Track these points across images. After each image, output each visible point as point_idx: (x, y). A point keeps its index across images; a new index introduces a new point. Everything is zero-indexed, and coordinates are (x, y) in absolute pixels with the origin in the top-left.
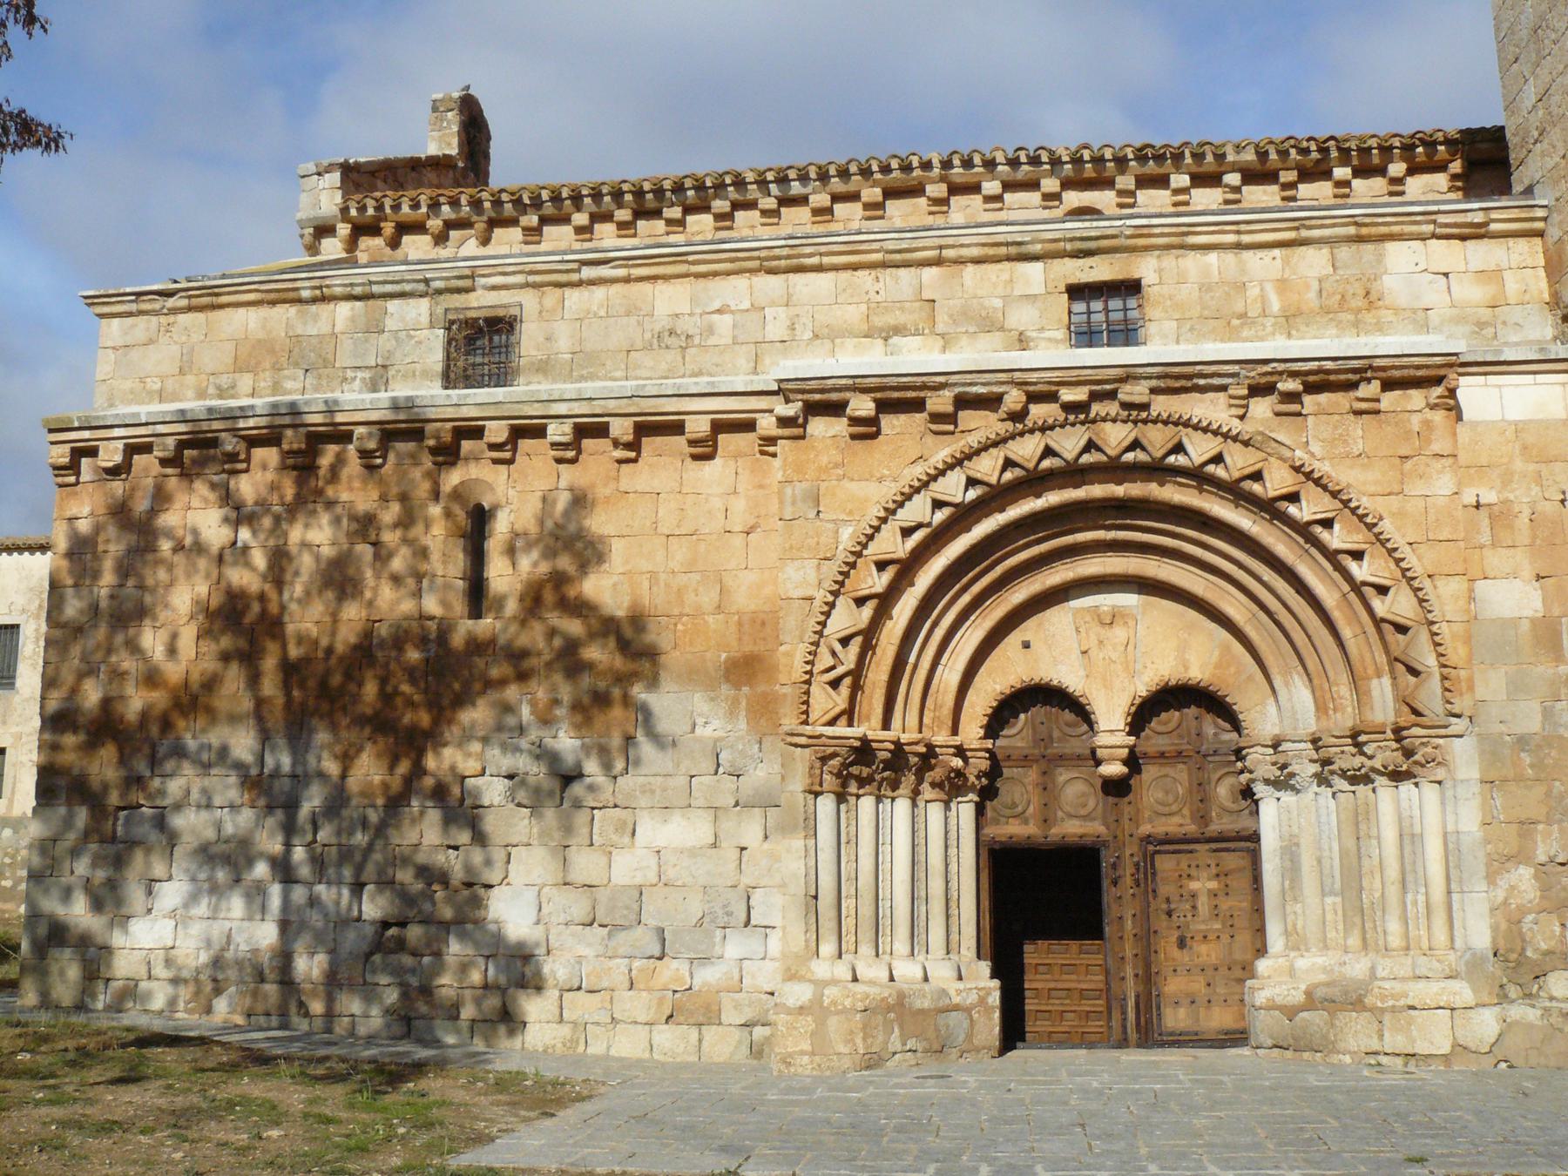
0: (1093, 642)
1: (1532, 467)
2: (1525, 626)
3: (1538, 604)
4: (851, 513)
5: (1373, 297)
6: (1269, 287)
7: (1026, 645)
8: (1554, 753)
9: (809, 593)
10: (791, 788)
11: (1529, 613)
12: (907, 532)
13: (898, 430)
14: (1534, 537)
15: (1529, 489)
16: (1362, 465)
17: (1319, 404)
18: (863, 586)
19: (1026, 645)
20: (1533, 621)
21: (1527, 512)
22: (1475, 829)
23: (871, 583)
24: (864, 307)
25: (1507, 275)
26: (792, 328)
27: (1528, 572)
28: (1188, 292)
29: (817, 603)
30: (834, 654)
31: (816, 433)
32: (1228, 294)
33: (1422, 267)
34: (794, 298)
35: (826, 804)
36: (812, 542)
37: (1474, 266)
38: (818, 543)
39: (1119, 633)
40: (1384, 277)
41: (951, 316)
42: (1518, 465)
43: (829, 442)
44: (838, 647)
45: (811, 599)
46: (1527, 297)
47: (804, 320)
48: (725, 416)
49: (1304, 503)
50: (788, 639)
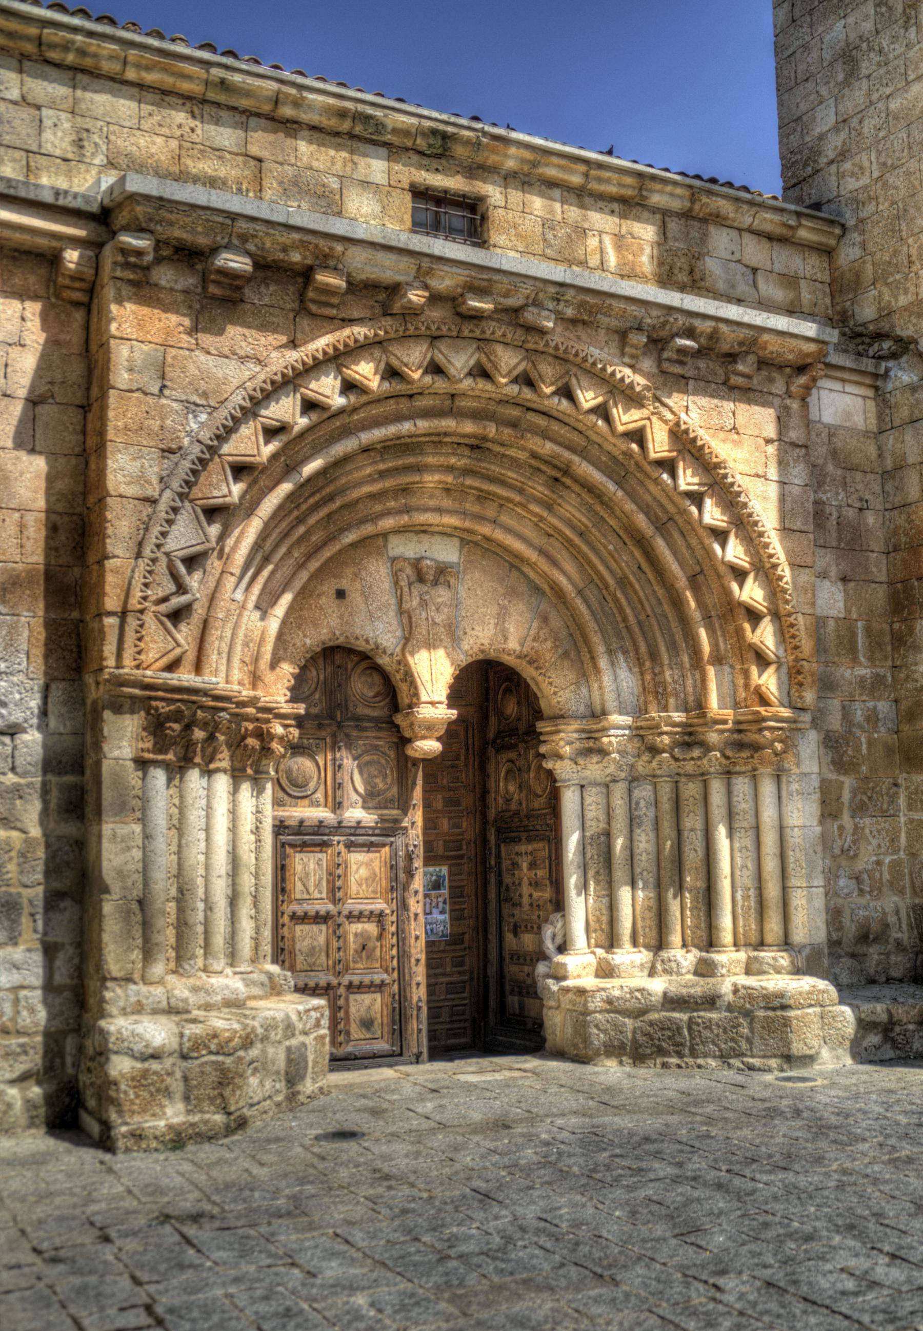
0: (415, 603)
1: (839, 472)
2: (831, 624)
3: (841, 605)
4: (205, 395)
5: (697, 276)
6: (608, 241)
7: (341, 594)
8: (850, 752)
9: (153, 490)
10: (116, 753)
11: (833, 613)
12: (271, 433)
13: (266, 300)
14: (840, 540)
15: (837, 493)
16: (734, 441)
17: (698, 368)
18: (216, 493)
19: (341, 594)
20: (837, 619)
21: (835, 515)
22: (815, 823)
23: (225, 491)
24: (174, 144)
25: (803, 284)
26: (79, 144)
27: (833, 572)
28: (531, 225)
29: (163, 506)
30: (175, 577)
31: (163, 283)
32: (569, 236)
33: (737, 256)
34: (83, 106)
35: (159, 777)
36: (155, 424)
37: (778, 267)
38: (162, 428)
39: (442, 595)
40: (707, 259)
41: (280, 183)
42: (830, 468)
43: (180, 297)
44: (182, 569)
45: (153, 502)
46: (816, 311)
47: (96, 138)
48: (17, 236)
49: (681, 471)
50: (118, 552)
